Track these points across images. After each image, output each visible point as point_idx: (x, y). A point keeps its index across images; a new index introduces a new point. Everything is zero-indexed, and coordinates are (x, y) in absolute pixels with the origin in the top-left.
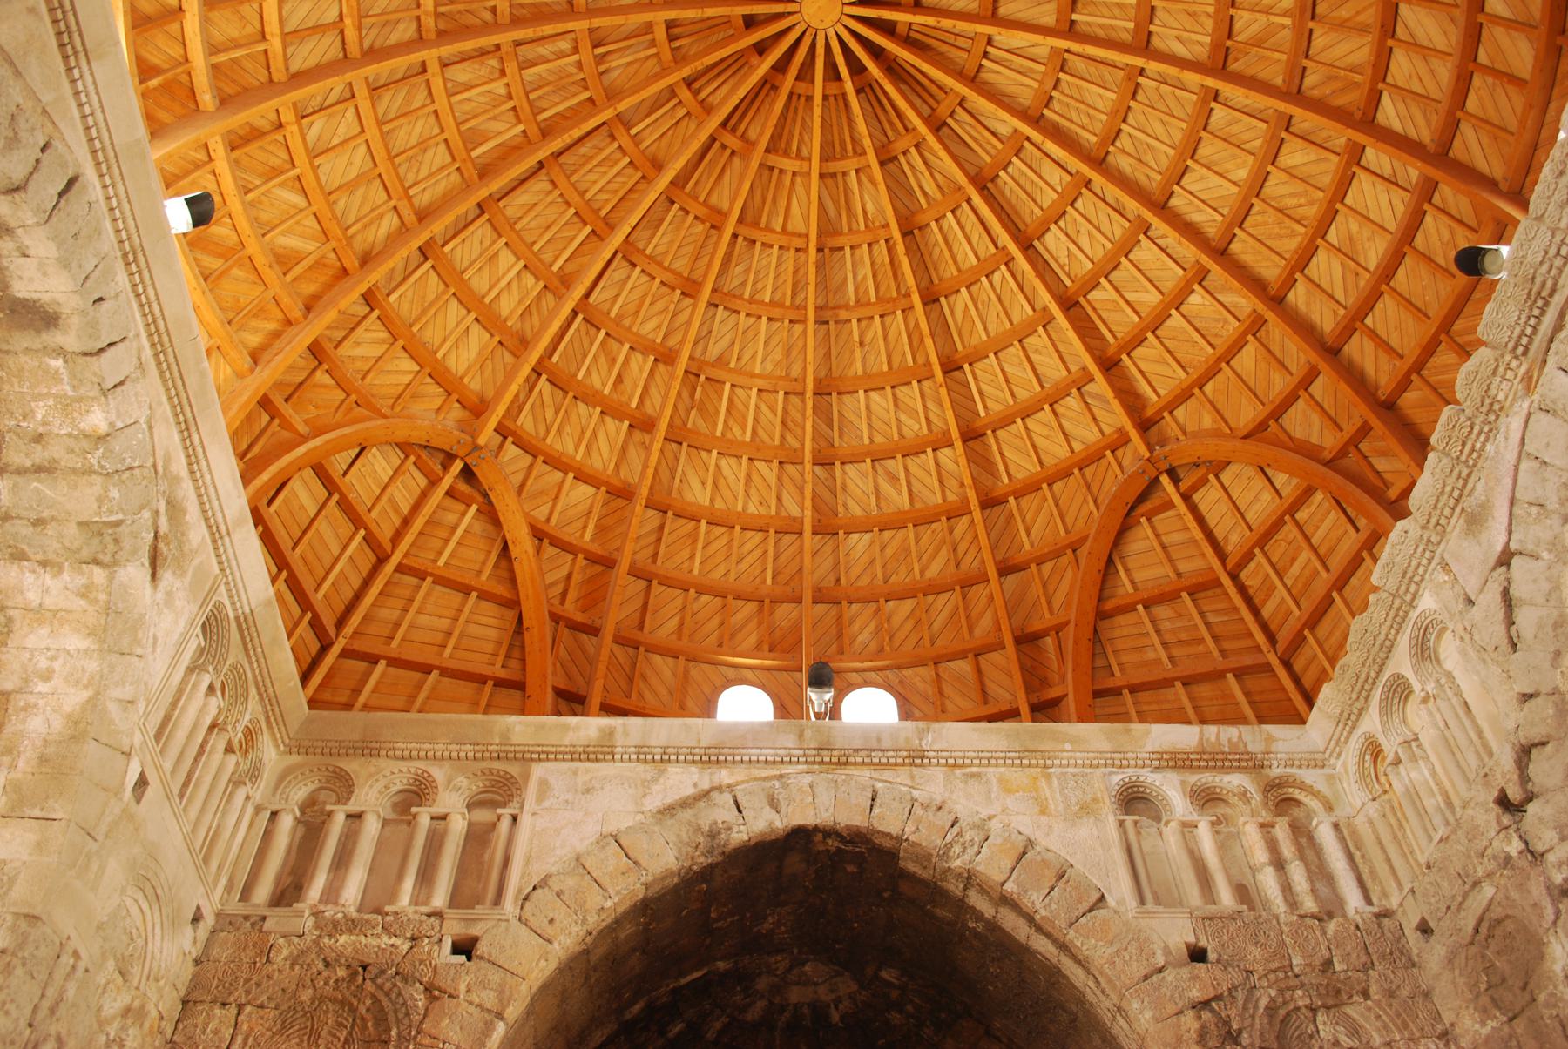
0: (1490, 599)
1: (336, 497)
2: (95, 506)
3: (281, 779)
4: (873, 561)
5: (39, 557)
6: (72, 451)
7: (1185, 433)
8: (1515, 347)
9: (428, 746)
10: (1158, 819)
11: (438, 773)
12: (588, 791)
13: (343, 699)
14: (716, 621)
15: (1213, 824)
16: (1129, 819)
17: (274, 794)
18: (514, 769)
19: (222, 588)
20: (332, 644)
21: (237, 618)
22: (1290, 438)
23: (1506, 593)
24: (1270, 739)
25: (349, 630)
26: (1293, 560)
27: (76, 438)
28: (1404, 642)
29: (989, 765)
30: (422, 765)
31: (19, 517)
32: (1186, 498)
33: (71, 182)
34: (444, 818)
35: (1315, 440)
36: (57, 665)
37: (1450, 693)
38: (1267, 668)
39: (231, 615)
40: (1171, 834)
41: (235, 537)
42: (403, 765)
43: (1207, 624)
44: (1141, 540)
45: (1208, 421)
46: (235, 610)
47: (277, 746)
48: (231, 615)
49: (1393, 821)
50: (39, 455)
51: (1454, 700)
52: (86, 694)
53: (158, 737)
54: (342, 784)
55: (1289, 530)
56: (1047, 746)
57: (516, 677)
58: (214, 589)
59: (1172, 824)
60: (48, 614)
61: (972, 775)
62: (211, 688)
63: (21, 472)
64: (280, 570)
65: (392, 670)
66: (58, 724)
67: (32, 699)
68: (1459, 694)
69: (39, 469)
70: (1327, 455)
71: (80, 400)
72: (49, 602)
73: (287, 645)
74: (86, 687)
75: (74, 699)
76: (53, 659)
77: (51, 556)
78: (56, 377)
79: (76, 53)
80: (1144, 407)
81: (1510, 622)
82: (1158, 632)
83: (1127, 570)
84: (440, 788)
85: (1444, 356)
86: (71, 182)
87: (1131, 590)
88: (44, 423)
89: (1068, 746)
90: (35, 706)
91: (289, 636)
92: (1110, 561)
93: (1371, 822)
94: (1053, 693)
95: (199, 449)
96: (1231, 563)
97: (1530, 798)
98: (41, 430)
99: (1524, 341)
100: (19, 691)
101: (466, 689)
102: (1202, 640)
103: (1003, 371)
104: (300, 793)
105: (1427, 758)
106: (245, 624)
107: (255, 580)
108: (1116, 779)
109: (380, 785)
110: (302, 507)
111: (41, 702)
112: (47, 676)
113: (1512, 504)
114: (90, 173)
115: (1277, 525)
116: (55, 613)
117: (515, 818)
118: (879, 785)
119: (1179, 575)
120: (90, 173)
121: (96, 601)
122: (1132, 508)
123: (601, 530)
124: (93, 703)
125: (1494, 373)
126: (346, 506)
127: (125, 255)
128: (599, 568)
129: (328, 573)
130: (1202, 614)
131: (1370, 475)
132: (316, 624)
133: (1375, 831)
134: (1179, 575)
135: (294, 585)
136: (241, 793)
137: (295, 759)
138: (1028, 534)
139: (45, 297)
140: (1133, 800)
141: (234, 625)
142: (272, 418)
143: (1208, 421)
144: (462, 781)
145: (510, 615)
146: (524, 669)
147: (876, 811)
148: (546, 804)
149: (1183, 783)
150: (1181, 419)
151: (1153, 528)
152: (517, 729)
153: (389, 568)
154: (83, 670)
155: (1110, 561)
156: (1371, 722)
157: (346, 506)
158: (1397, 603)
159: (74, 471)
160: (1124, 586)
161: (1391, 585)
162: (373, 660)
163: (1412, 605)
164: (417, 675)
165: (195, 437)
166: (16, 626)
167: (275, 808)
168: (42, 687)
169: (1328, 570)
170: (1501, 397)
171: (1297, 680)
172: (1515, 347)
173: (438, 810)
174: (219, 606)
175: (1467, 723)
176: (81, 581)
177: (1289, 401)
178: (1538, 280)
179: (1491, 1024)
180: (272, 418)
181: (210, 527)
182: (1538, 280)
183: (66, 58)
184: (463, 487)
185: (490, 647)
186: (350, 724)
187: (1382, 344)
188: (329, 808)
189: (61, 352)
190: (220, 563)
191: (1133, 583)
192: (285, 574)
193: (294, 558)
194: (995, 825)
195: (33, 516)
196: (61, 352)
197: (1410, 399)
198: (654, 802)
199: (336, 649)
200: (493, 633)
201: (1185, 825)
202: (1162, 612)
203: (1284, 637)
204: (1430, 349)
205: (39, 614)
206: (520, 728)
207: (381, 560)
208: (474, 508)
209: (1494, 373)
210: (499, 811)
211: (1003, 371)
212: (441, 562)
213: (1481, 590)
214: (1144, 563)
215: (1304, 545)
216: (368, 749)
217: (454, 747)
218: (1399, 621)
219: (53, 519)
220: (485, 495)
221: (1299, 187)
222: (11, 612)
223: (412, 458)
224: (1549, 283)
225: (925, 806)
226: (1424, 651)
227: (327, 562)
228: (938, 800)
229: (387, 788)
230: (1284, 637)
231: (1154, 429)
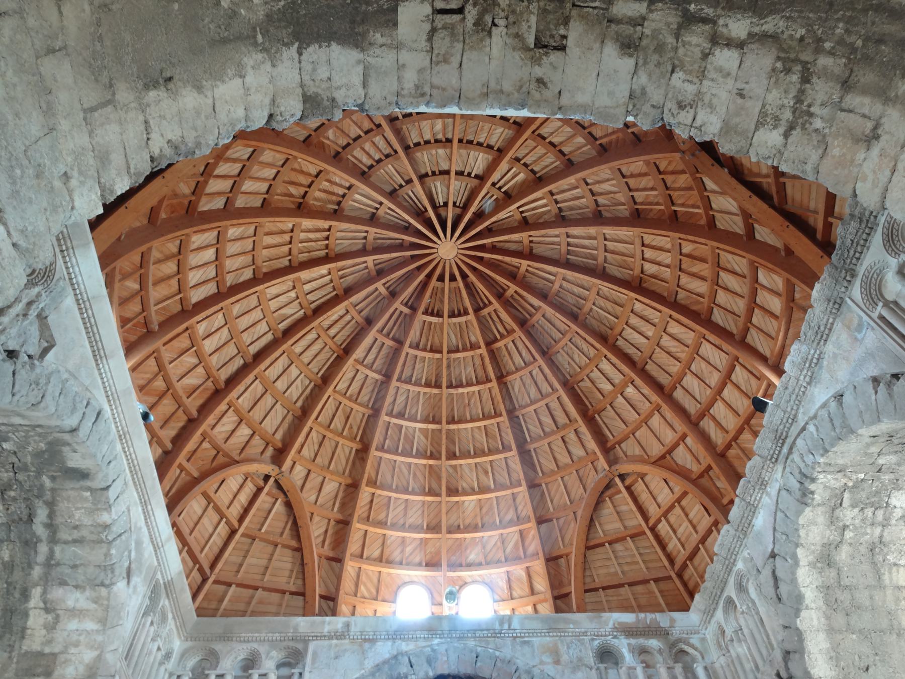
0: (767, 573)
1: (212, 504)
2: (103, 558)
3: (183, 655)
4: (476, 516)
5: (74, 584)
6: (92, 533)
7: (626, 456)
8: (772, 457)
9: (257, 635)
10: (617, 664)
11: (262, 649)
12: (336, 658)
13: (213, 606)
14: (399, 550)
15: (644, 668)
16: (602, 666)
17: (179, 665)
18: (300, 646)
19: (159, 573)
20: (208, 578)
21: (164, 583)
22: (677, 464)
23: (774, 572)
24: (673, 621)
25: (217, 570)
26: (680, 525)
27: (95, 526)
28: (732, 581)
29: (533, 636)
30: (255, 645)
32: (628, 488)
33: (99, 414)
34: (265, 675)
35: (688, 466)
36: (82, 638)
37: (753, 612)
38: (670, 578)
39: (162, 582)
40: (623, 671)
41: (166, 547)
42: (245, 646)
43: (640, 554)
44: (608, 509)
45: (637, 451)
46: (164, 579)
47: (180, 638)
48: (162, 582)
49: (733, 668)
50: (76, 535)
51: (756, 617)
52: (96, 653)
53: (126, 658)
54: (212, 658)
55: (677, 510)
56: (561, 626)
57: (301, 590)
58: (155, 574)
59: (624, 668)
60: (78, 612)
61: (525, 642)
62: (152, 623)
63: (66, 542)
64: (184, 546)
65: (239, 589)
66: (81, 669)
67: (69, 657)
68: (758, 613)
69: (75, 541)
70: (694, 476)
71: (98, 509)
72: (78, 606)
73: (186, 582)
74: (96, 649)
75: (89, 656)
76: (80, 635)
77: (80, 583)
78: (86, 499)
79: (101, 358)
80: (607, 441)
81: (777, 587)
82: (616, 557)
83: (600, 524)
84: (263, 657)
85: (746, 436)
86: (99, 414)
87: (602, 535)
88: (79, 520)
89: (571, 626)
90: (70, 660)
91: (187, 578)
92: (592, 520)
93: (722, 667)
94: (565, 591)
95: (151, 512)
96: (652, 522)
99: (775, 456)
100: (62, 653)
101: (276, 597)
103: (539, 420)
104: (191, 663)
105: (746, 641)
106: (169, 586)
107: (173, 561)
108: (596, 643)
109: (232, 658)
110: (195, 512)
111: (73, 658)
112: (77, 644)
114: (106, 407)
115: (672, 507)
116: (81, 611)
117: (301, 674)
118: (479, 649)
119: (625, 527)
120: (106, 407)
121: (102, 604)
122: (602, 493)
123: (343, 505)
124: (99, 658)
125: (763, 468)
126: (217, 509)
127: (120, 436)
128: (341, 526)
129: (207, 542)
130: (637, 548)
131: (714, 489)
132: (201, 570)
133: (724, 672)
134: (625, 527)
135: (191, 553)
136: (162, 669)
137: (189, 644)
138: (552, 502)
139: (84, 467)
140: (606, 655)
141: (163, 586)
142: (181, 471)
143: (637, 451)
144: (274, 653)
145: (298, 554)
146: (304, 585)
147: (479, 664)
148: (316, 665)
149: (629, 645)
150: (625, 449)
151: (612, 503)
152: (302, 624)
153: (237, 536)
154: (95, 640)
155: (592, 520)
157: (217, 509)
158: (727, 562)
159: (93, 541)
160: (600, 534)
161: (723, 553)
162: (229, 585)
164: (251, 591)
165: (149, 507)
166: (62, 618)
167: (179, 674)
168: (73, 650)
169: (697, 532)
170: (766, 479)
171: (685, 585)
172: (772, 457)
173: (262, 671)
174: (157, 582)
175: (762, 630)
176: (94, 594)
177: (675, 446)
178: (779, 432)
180: (181, 471)
181: (154, 545)
182: (779, 432)
183: (96, 360)
184: (275, 491)
185: (287, 573)
186: (217, 624)
187: (718, 424)
188: (207, 672)
189: (89, 489)
190: (158, 560)
191: (603, 531)
192: (186, 548)
193: (191, 540)
194: (536, 671)
195: (72, 563)
196: (89, 489)
197: (732, 453)
198: (369, 664)
199: (210, 581)
200: (289, 566)
201: (630, 668)
202: (618, 547)
203: (679, 562)
204: (740, 431)
205: (75, 613)
206: (303, 624)
207: (233, 532)
208: (279, 501)
209: (763, 468)
210: (293, 671)
211: (539, 420)
212: (263, 531)
213: (763, 568)
214: (608, 524)
215: (685, 518)
216: (226, 637)
217: (270, 635)
219: (82, 564)
220: (285, 493)
221: (677, 344)
222: (59, 612)
223: (249, 479)
224: (784, 434)
225: (503, 661)
226: (741, 588)
227: (207, 536)
228: (508, 657)
229: (236, 658)
230: (679, 562)
231: (612, 453)
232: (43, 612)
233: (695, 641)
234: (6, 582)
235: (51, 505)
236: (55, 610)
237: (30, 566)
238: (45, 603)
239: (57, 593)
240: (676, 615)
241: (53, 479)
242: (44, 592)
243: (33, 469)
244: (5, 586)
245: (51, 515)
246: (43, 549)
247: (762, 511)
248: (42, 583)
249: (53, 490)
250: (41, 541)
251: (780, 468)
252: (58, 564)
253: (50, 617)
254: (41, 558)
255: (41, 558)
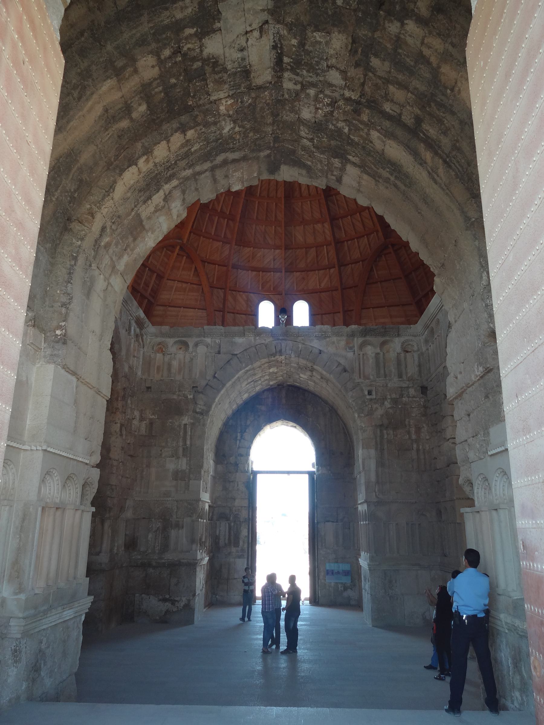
31: (197, 184)
97: (202, 393)
98: (230, 176)
102: (148, 287)
113: (245, 350)
139: (281, 172)
156: (170, 341)
163: (204, 337)
179: (153, 416)
218: (199, 336)
222: (166, 205)
226: (196, 345)
232: (163, 197)
233: (145, 337)
234: (176, 162)
235: (244, 158)
236: (167, 202)
237: (190, 167)
238: (170, 193)
239: (177, 194)
240: (150, 325)
241: (268, 156)
242: (175, 187)
243: (276, 145)
244: (173, 162)
245: (234, 161)
246: (207, 165)
247: (244, 339)
248: (181, 181)
249: (257, 158)
250: (212, 162)
251: (271, 339)
252: (196, 180)
253: (162, 203)
254: (198, 168)
255: (198, 168)
